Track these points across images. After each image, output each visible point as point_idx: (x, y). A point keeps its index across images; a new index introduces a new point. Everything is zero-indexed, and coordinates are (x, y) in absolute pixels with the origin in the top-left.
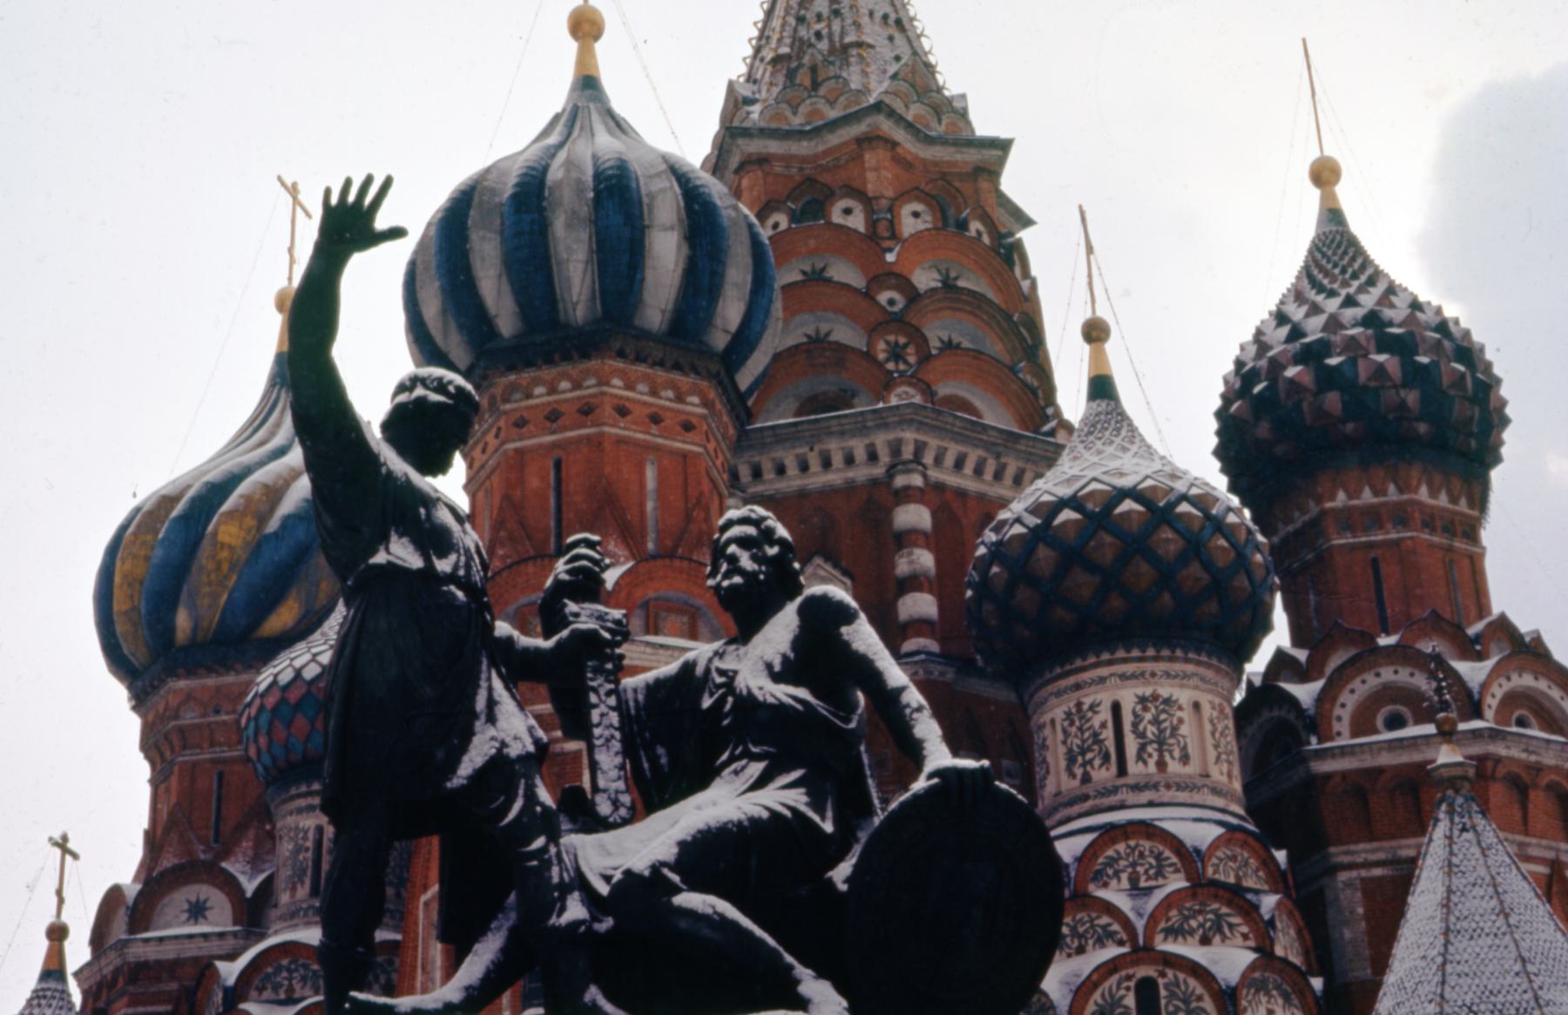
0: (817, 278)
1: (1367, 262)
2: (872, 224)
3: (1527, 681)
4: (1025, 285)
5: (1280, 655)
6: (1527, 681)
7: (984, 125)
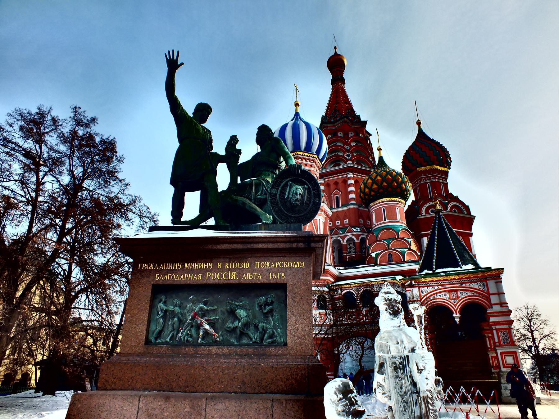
2: (344, 134)
3: (455, 203)
6: (455, 203)
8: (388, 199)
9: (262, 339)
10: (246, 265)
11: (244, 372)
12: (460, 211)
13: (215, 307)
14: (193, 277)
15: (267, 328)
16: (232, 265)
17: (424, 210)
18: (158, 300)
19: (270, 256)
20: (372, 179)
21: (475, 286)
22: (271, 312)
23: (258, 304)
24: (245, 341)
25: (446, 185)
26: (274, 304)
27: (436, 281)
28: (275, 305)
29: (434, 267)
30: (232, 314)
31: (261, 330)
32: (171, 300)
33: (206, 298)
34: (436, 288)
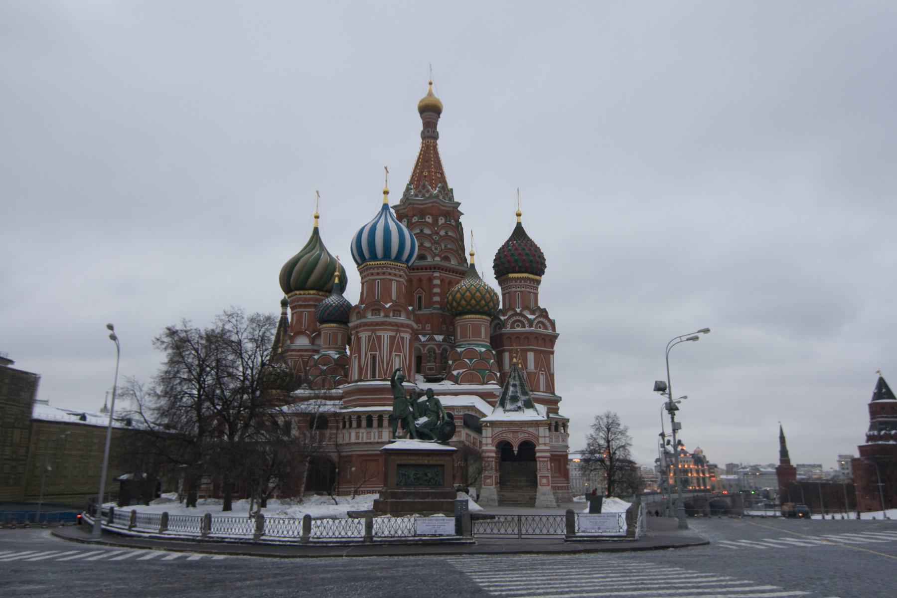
0: (422, 231)
2: (433, 221)
3: (541, 319)
6: (541, 319)
12: (546, 328)
21: (531, 430)
25: (536, 295)
30: (426, 475)
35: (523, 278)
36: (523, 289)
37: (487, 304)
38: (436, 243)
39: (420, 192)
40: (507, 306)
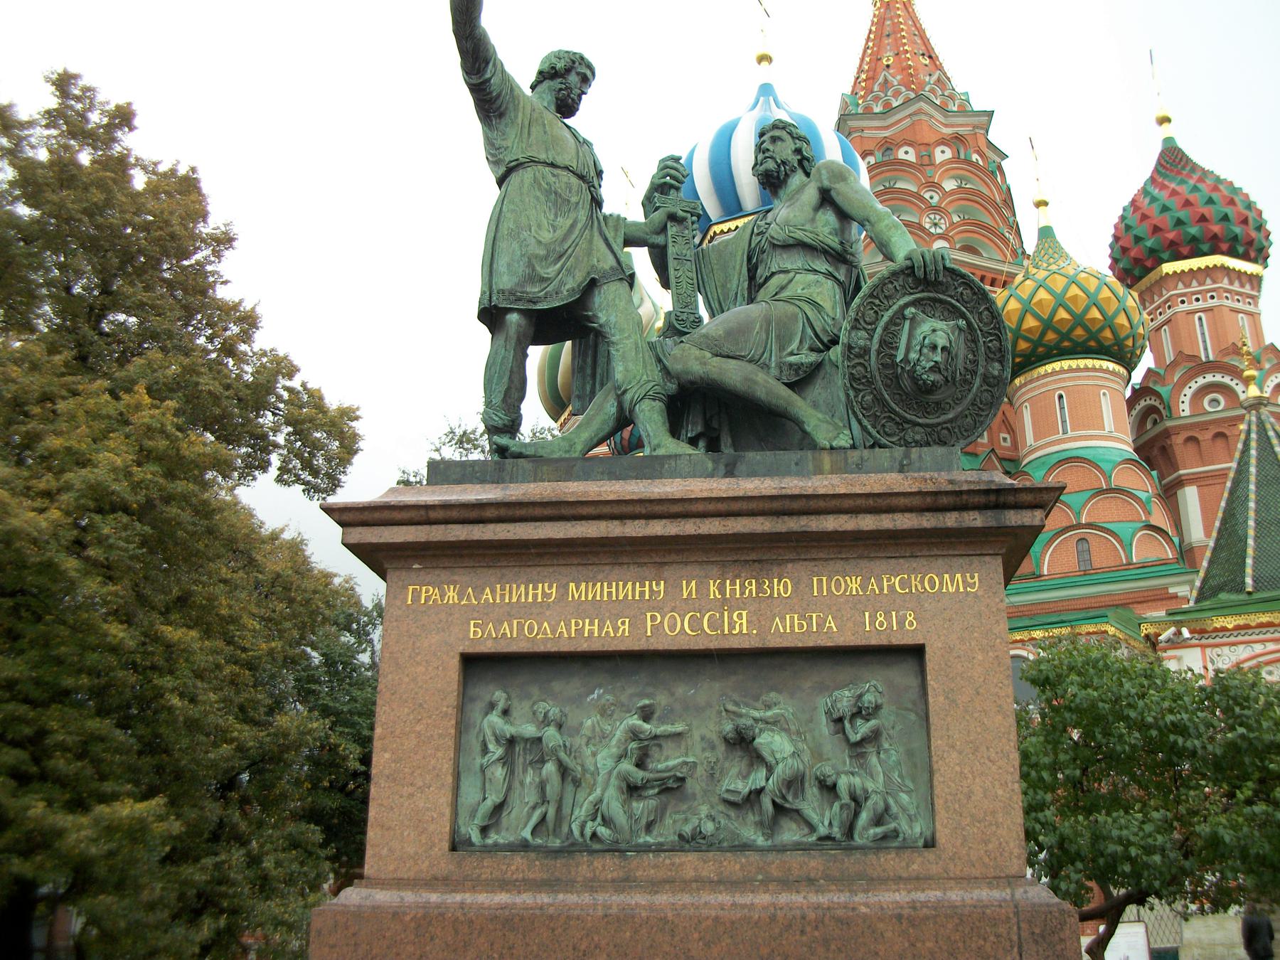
1: (1188, 159)
2: (919, 156)
4: (1004, 188)
5: (1149, 370)
7: (978, 103)
8: (1073, 364)
9: (849, 831)
10: (781, 587)
11: (803, 932)
13: (679, 727)
14: (601, 628)
15: (866, 791)
16: (733, 588)
17: (1187, 400)
18: (479, 706)
19: (860, 557)
20: (1019, 300)
22: (874, 737)
23: (828, 713)
24: (790, 833)
26: (884, 712)
27: (1261, 625)
28: (885, 719)
29: (1249, 581)
30: (742, 743)
31: (846, 799)
32: (526, 705)
33: (648, 696)
34: (1258, 648)
35: (1208, 271)
36: (1211, 303)
37: (1109, 323)
38: (936, 209)
39: (877, 99)
40: (1169, 357)
